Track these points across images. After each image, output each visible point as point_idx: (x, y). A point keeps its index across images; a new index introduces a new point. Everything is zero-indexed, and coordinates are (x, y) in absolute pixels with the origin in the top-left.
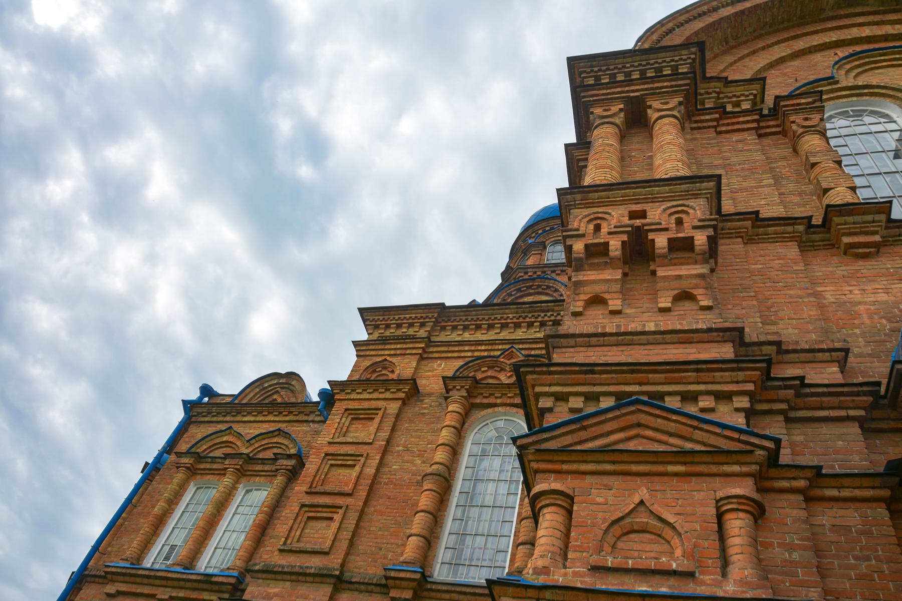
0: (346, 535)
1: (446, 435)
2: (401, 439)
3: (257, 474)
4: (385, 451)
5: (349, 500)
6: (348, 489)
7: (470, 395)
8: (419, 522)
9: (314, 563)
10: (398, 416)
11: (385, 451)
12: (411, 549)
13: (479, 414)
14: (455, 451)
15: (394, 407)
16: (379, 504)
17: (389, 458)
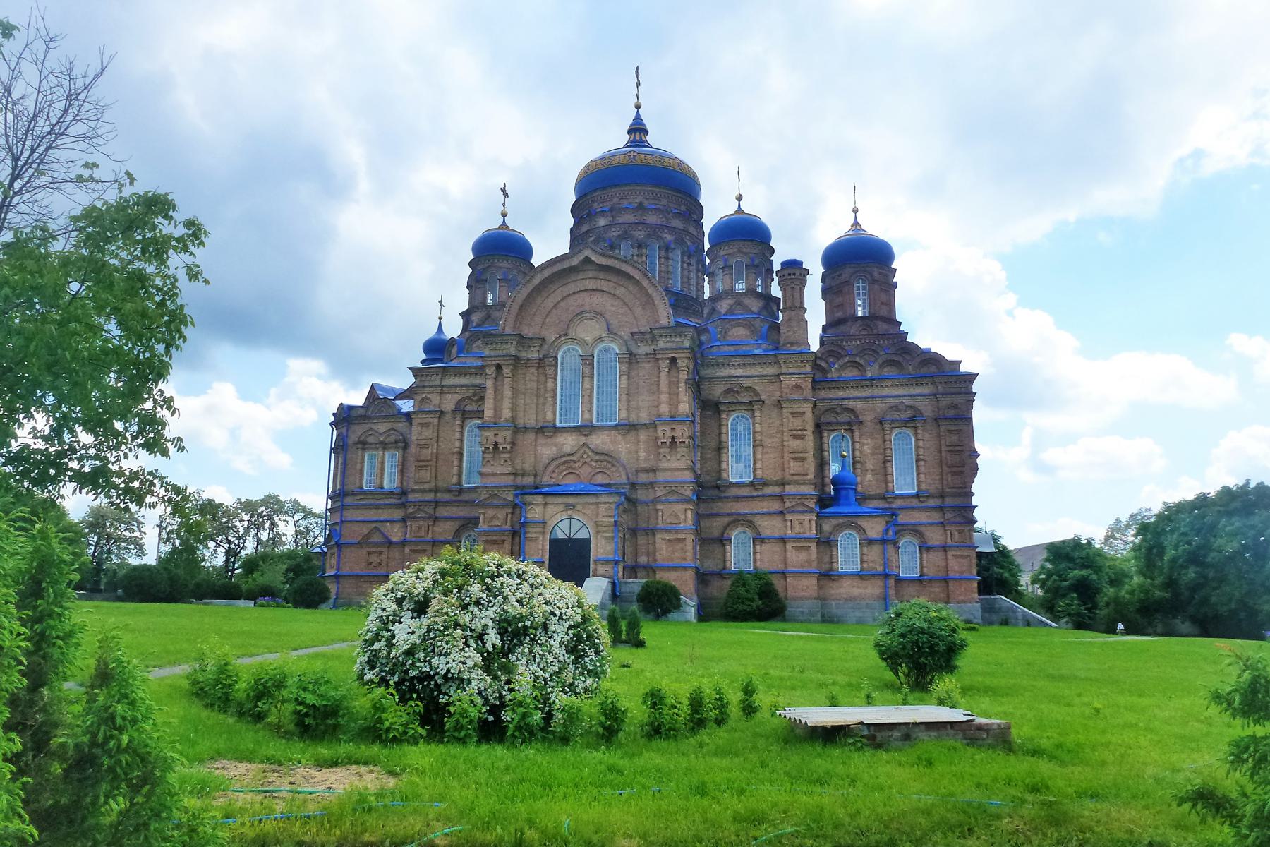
0: (434, 475)
1: (457, 435)
2: (442, 434)
3: (390, 448)
4: (437, 441)
5: (430, 463)
6: (429, 458)
7: (462, 415)
8: (455, 470)
9: (426, 486)
10: (438, 425)
11: (437, 441)
12: (455, 479)
13: (467, 422)
14: (461, 440)
15: (436, 421)
16: (440, 463)
17: (440, 443)
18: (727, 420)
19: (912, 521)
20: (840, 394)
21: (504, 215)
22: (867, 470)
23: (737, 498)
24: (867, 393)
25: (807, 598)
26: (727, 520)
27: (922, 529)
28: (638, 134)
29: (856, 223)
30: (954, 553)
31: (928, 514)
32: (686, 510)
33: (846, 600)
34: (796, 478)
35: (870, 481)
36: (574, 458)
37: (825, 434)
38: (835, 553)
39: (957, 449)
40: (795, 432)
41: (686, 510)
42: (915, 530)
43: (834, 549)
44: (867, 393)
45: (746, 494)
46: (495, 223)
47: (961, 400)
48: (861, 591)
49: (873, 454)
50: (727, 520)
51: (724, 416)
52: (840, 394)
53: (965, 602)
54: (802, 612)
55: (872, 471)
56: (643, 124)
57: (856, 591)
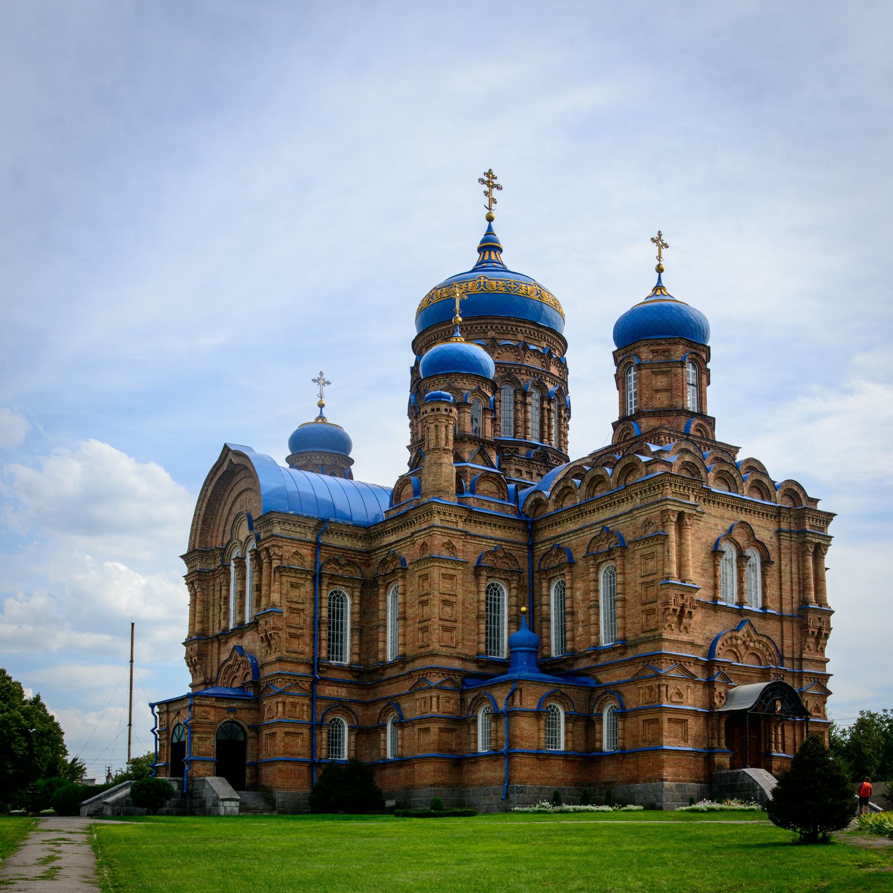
18: (386, 593)
19: (615, 681)
20: (560, 530)
21: (321, 406)
22: (579, 623)
23: (390, 680)
24: (579, 524)
25: (425, 786)
26: (383, 705)
27: (622, 689)
28: (487, 253)
29: (659, 287)
30: (644, 717)
31: (627, 669)
32: (277, 703)
33: (482, 785)
34: (423, 650)
35: (581, 635)
36: (231, 662)
37: (545, 584)
38: (472, 732)
39: (650, 578)
40: (447, 597)
41: (277, 703)
42: (613, 690)
43: (472, 727)
44: (579, 524)
45: (396, 674)
46: (310, 416)
47: (655, 512)
48: (493, 774)
49: (583, 601)
50: (383, 705)
51: (382, 591)
52: (560, 530)
53: (650, 780)
54: (421, 802)
55: (583, 622)
56: (497, 242)
57: (489, 775)
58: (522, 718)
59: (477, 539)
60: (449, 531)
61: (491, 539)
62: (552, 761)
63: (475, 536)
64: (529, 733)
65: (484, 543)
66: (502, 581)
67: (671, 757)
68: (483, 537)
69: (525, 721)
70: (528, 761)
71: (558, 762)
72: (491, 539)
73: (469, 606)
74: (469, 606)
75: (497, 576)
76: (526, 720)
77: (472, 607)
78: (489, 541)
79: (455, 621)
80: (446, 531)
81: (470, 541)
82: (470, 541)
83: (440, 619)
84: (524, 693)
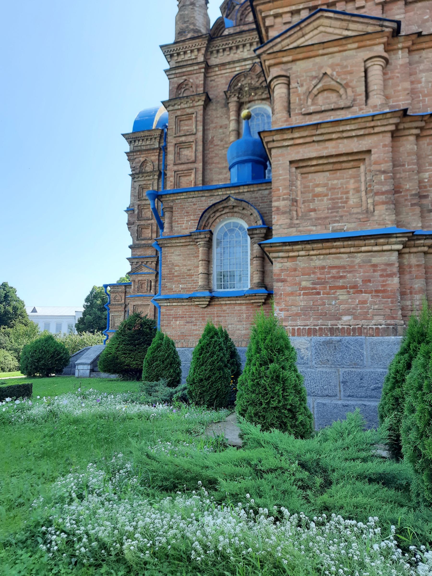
58: (172, 250)
59: (227, 67)
60: (184, 70)
61: (245, 60)
62: (225, 308)
63: (223, 64)
64: (184, 269)
65: (237, 69)
66: (264, 102)
67: (302, 263)
68: (234, 62)
69: (177, 253)
70: (180, 311)
71: (237, 308)
72: (245, 60)
73: (219, 143)
74: (219, 143)
75: (256, 98)
76: (177, 251)
77: (222, 143)
78: (243, 63)
79: (194, 162)
80: (180, 71)
81: (218, 73)
82: (218, 73)
83: (175, 164)
84: (175, 214)
